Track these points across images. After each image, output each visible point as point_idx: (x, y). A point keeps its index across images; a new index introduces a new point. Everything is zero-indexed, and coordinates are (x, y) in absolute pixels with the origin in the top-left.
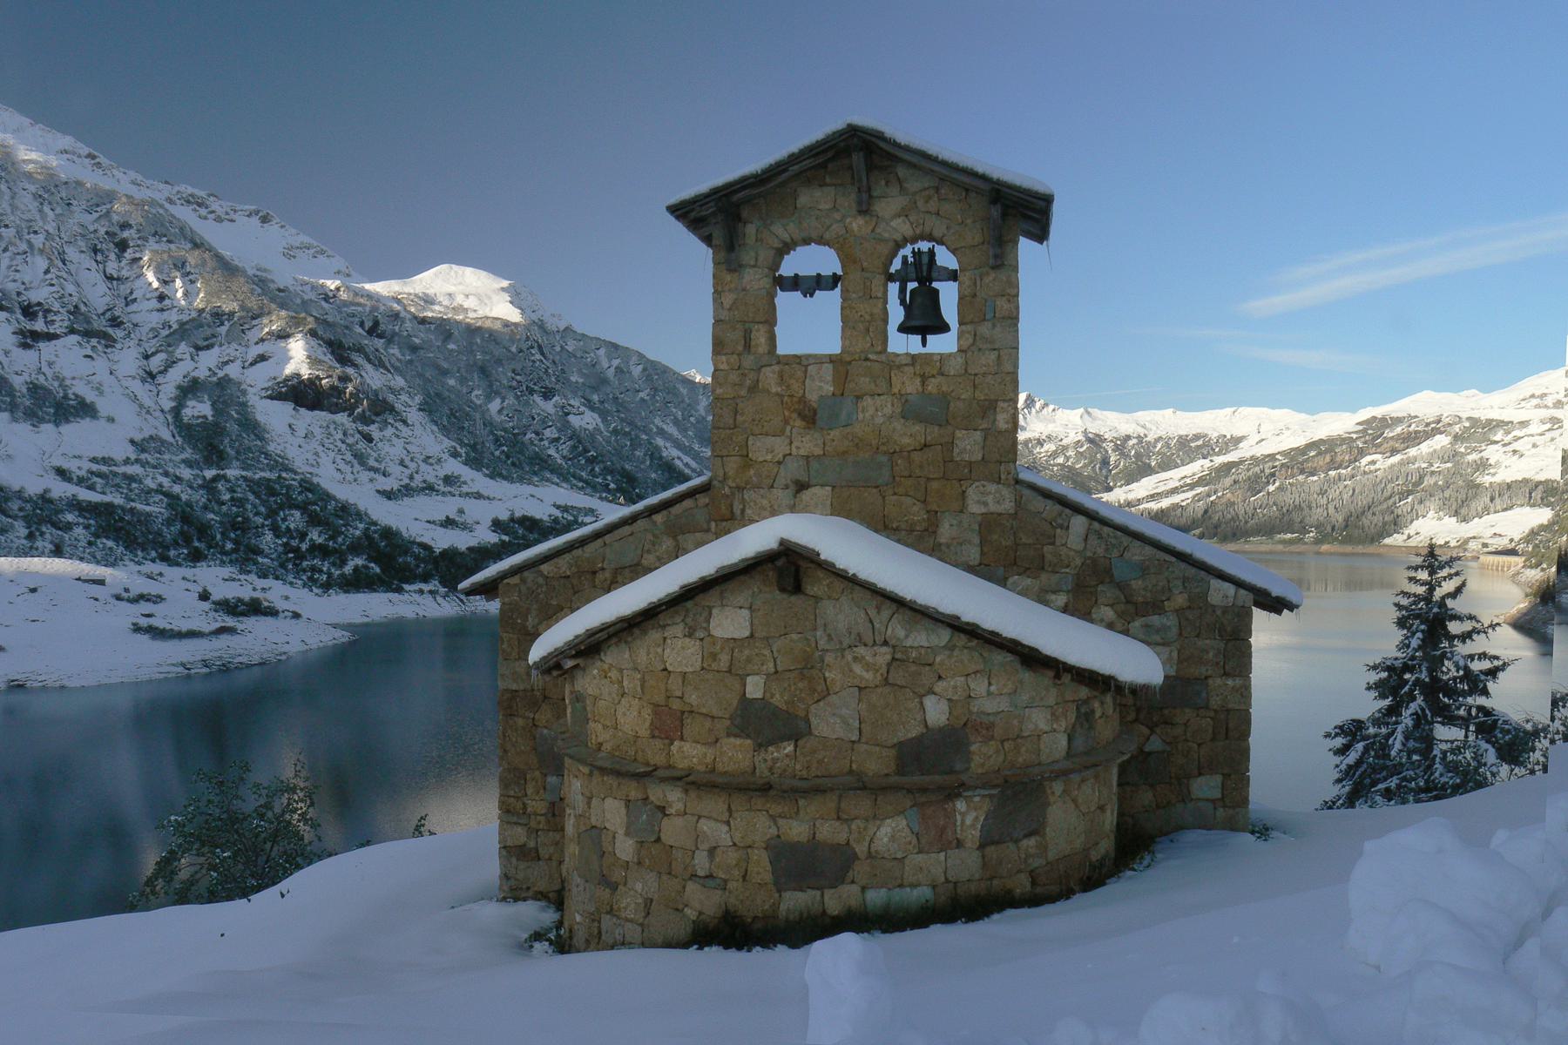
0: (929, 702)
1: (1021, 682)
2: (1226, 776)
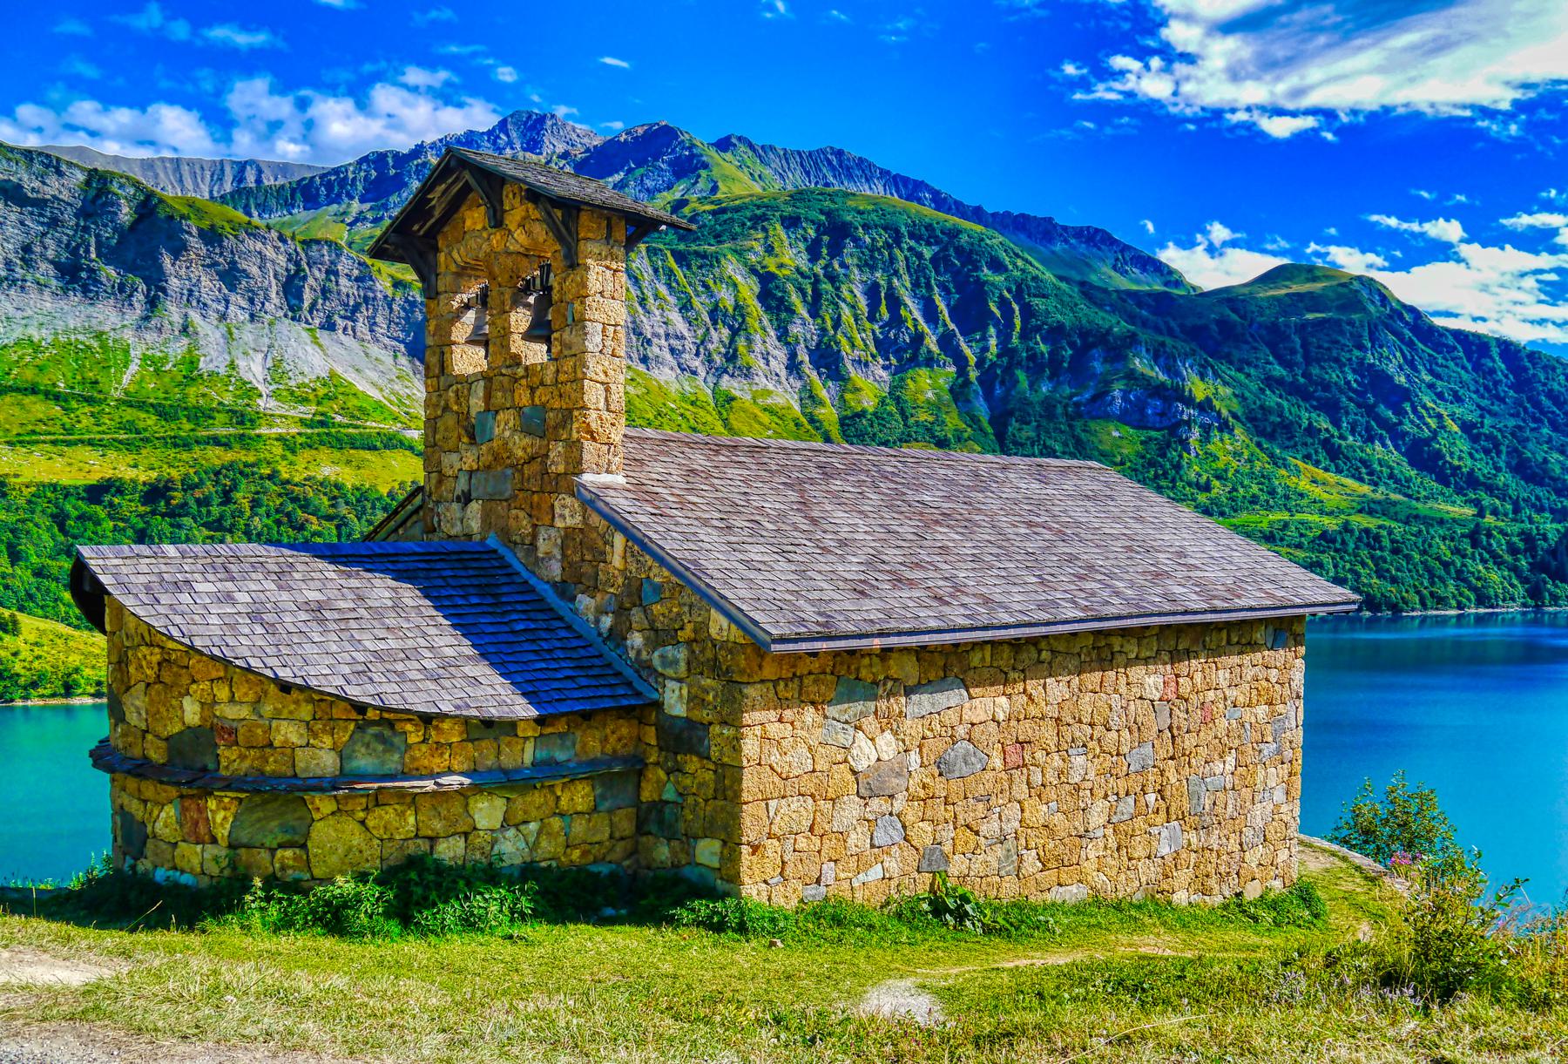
0: (187, 702)
1: (266, 693)
2: (725, 843)
